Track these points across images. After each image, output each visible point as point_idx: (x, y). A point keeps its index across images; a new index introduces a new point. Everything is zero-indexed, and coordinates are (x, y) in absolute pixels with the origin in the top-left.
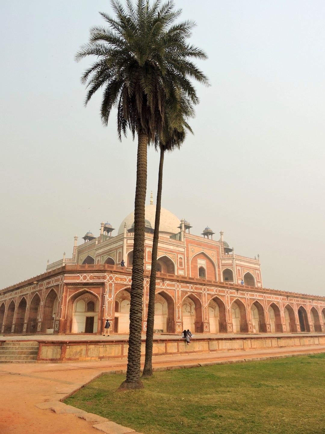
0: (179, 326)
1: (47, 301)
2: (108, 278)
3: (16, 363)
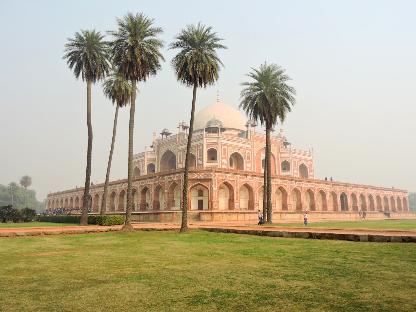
1: (170, 190)
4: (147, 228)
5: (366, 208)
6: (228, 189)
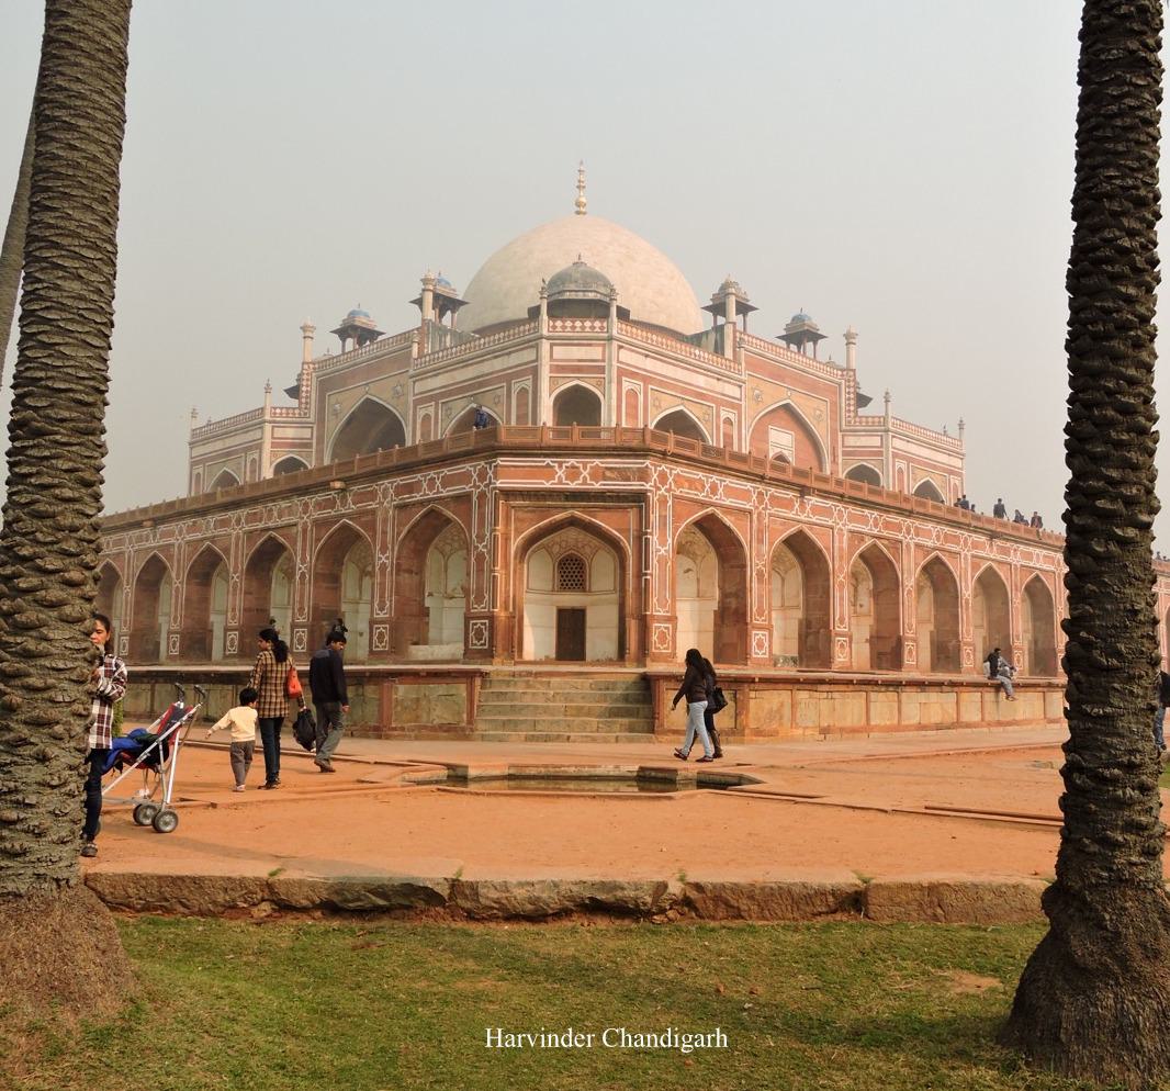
0: (842, 645)
1: (405, 552)
2: (655, 476)
3: (582, 742)
4: (341, 888)
6: (713, 559)
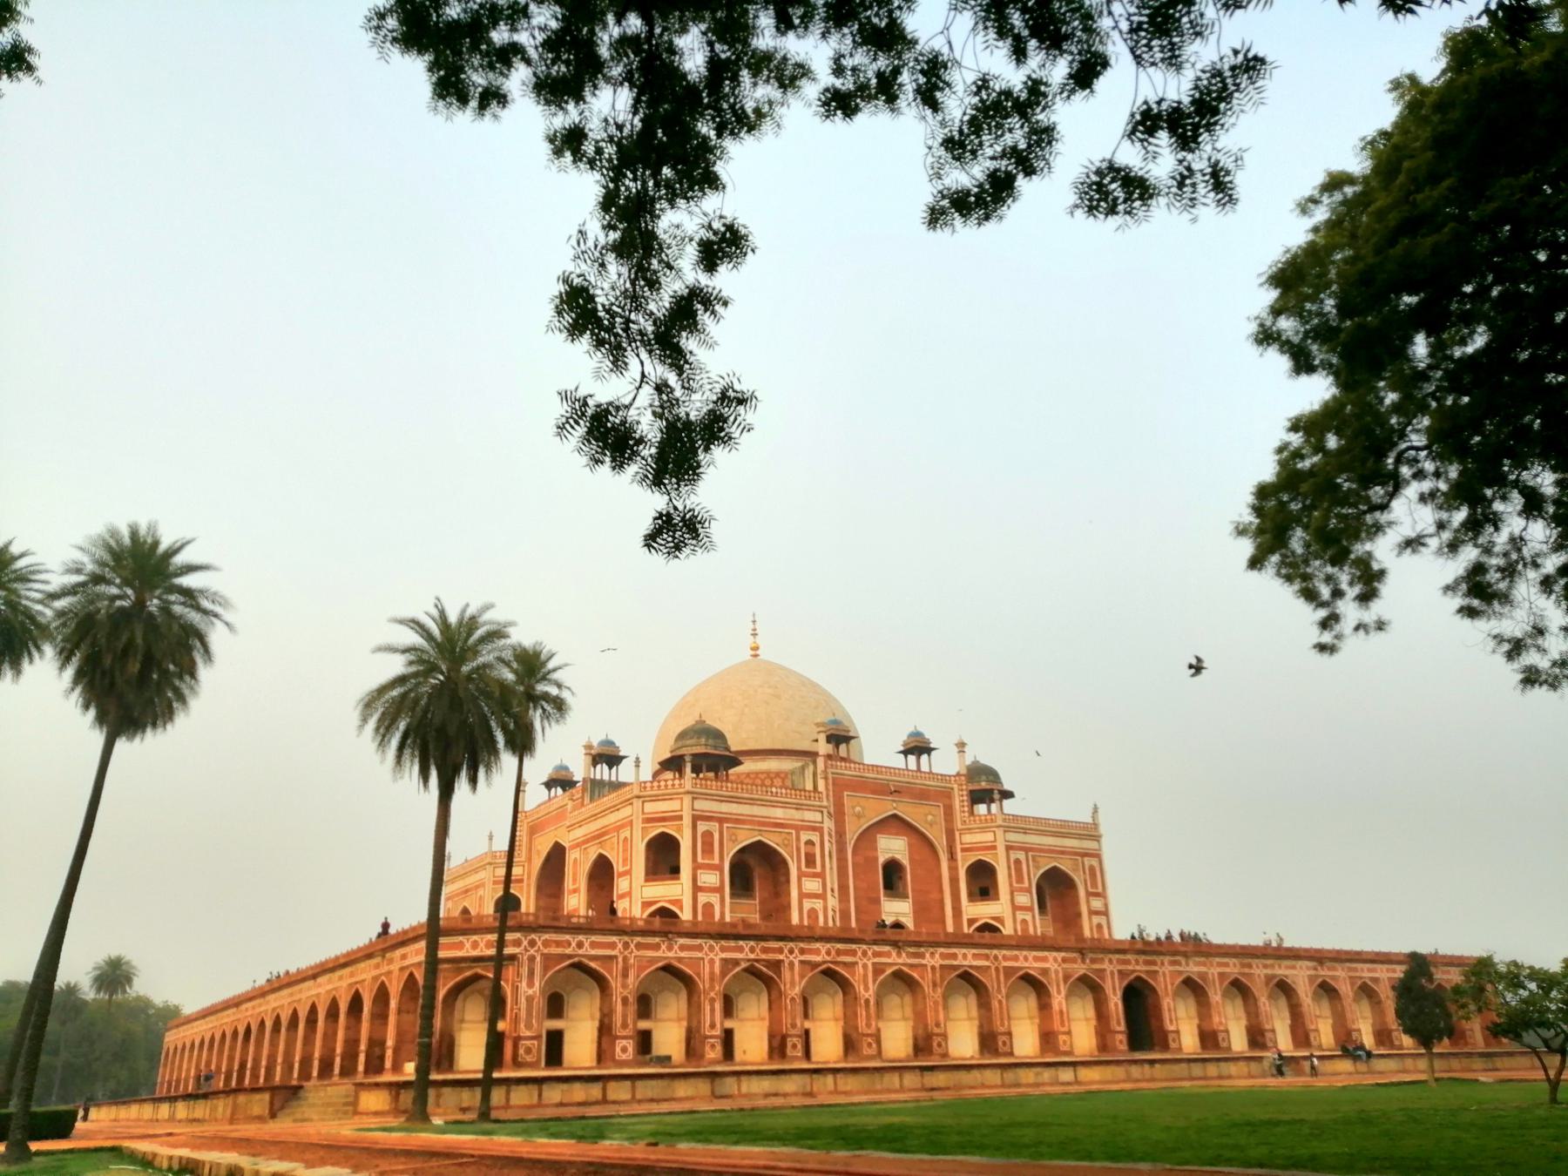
5: (1263, 1035)
